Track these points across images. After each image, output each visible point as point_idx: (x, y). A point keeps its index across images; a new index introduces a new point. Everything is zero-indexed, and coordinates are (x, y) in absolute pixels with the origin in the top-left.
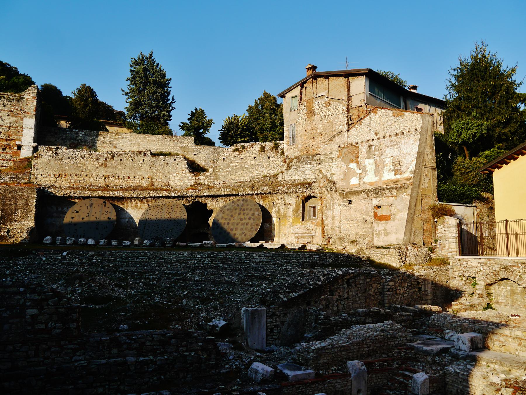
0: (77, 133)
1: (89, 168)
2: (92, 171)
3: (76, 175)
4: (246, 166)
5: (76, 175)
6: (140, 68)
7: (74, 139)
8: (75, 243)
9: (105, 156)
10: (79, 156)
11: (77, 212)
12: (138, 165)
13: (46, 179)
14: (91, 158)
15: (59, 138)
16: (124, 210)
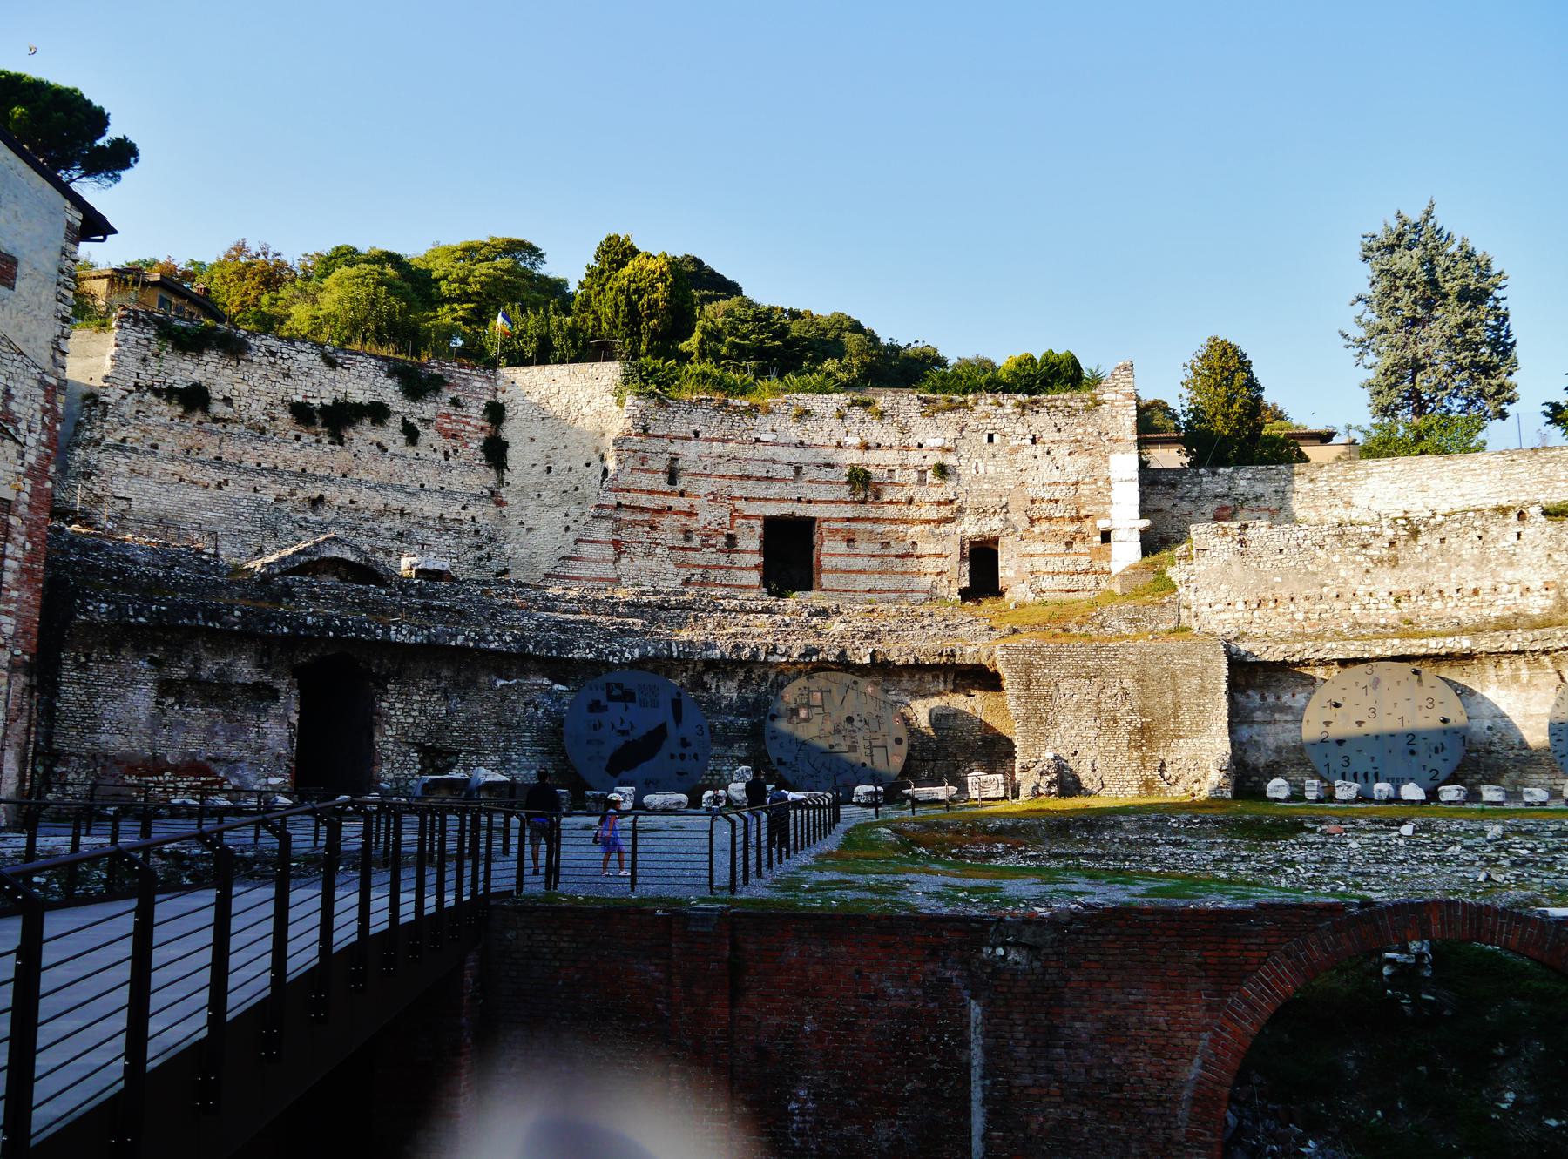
0: (1231, 478)
1: (1342, 573)
2: (1354, 583)
3: (1307, 598)
5: (1307, 598)
6: (1405, 261)
7: (1225, 496)
8: (1364, 797)
9: (1389, 533)
10: (1308, 542)
11: (1337, 705)
12: (1503, 552)
13: (1223, 616)
14: (1345, 546)
15: (1182, 499)
16: (1472, 693)
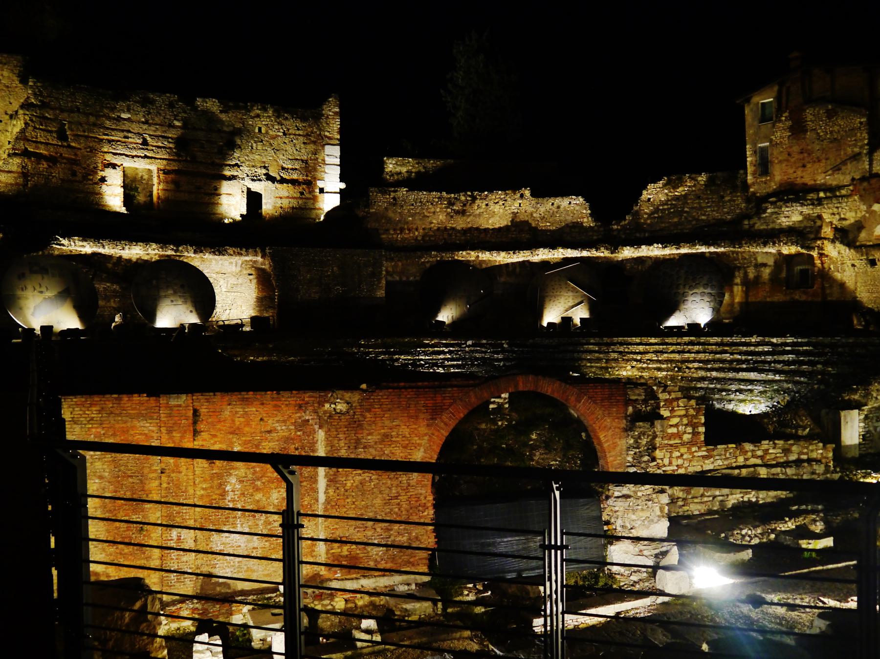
4: (686, 209)
